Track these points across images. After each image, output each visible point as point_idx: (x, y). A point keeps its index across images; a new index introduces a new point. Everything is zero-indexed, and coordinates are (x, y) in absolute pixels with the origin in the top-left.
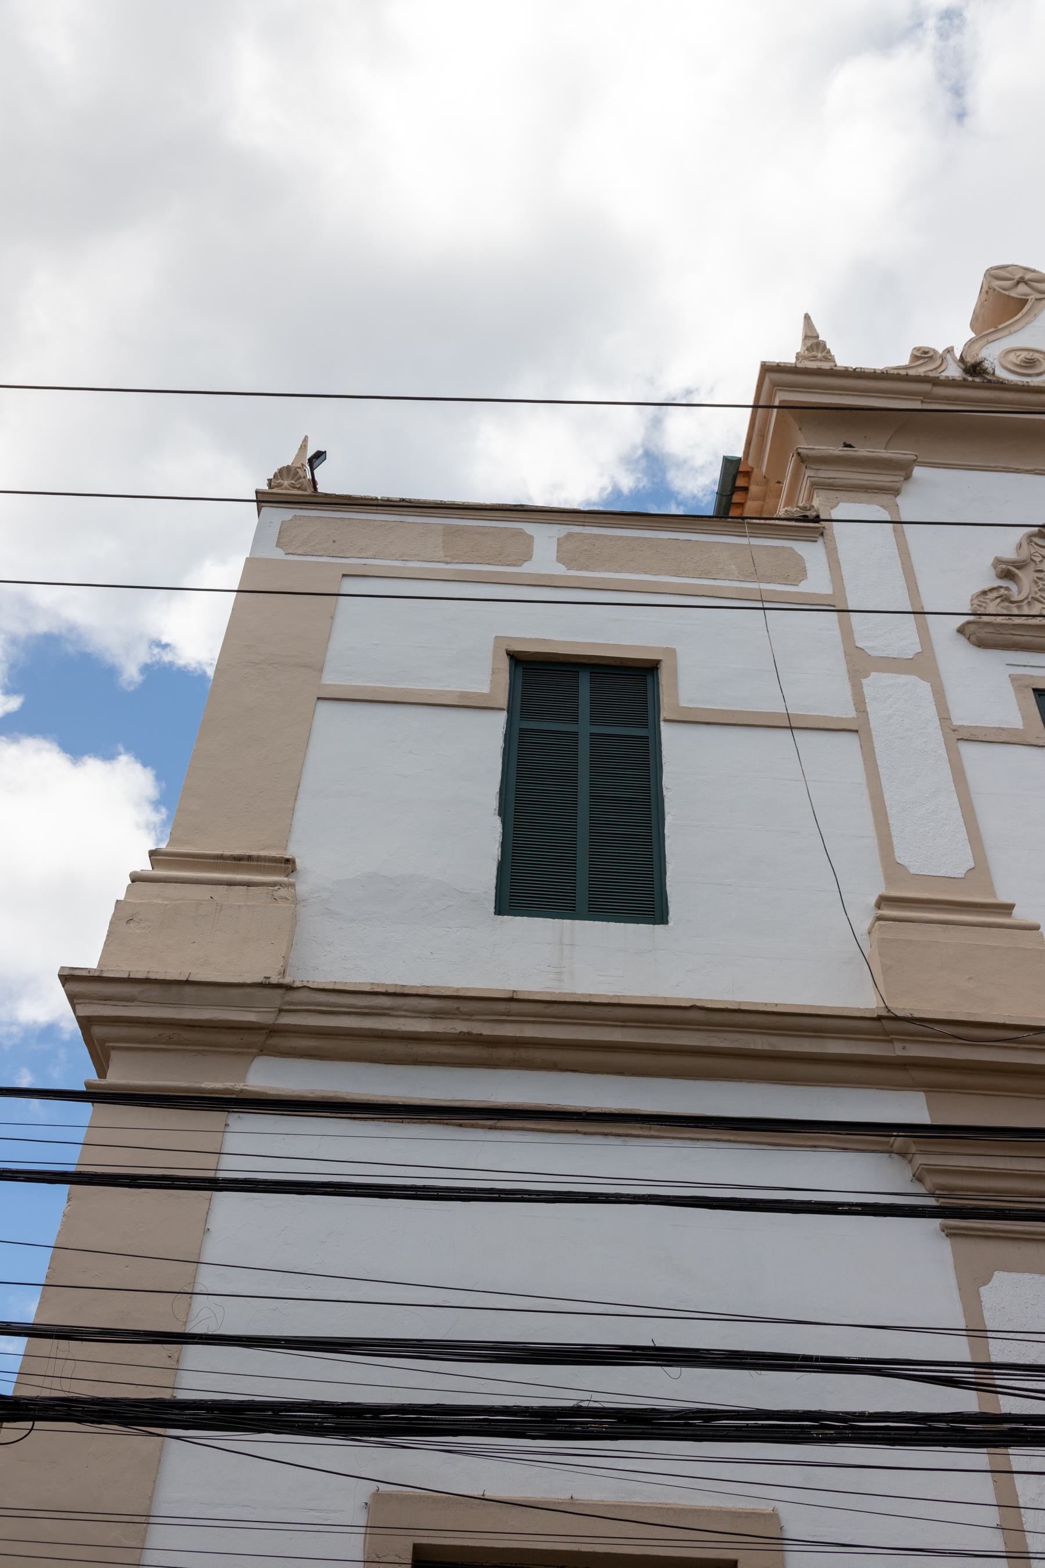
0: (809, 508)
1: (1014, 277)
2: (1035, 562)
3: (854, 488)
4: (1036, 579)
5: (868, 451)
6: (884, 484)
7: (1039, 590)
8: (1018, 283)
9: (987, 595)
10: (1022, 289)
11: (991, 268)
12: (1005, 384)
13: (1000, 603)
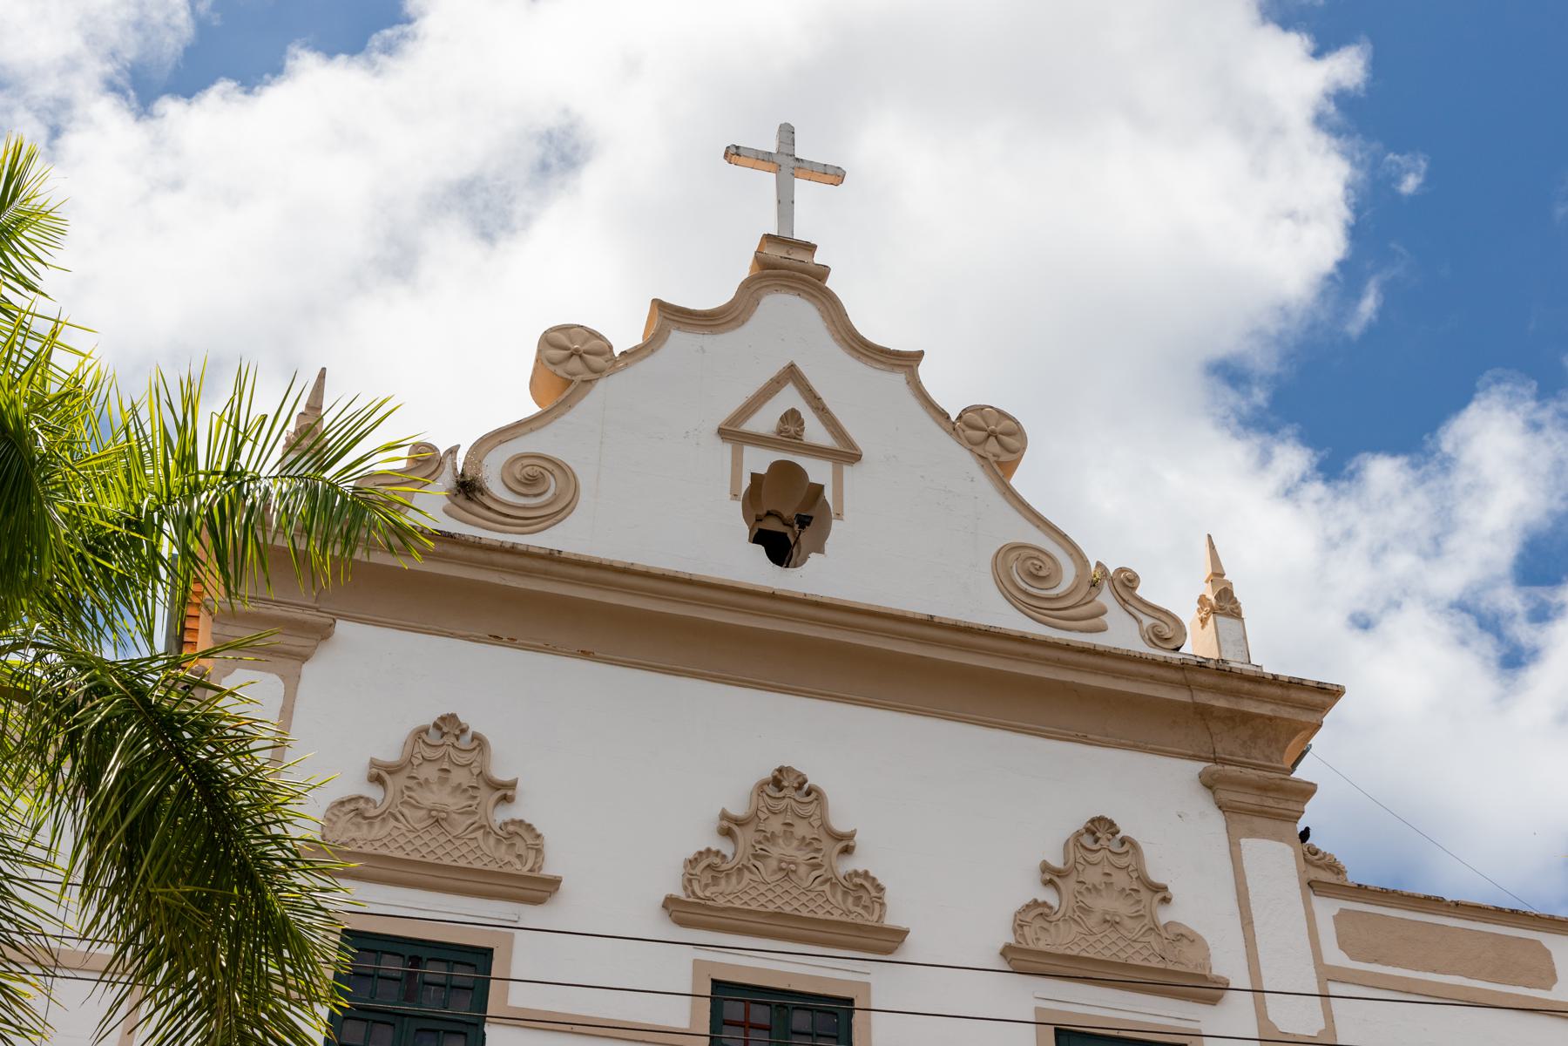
1: (570, 346)
2: (413, 765)
4: (404, 788)
5: (282, 610)
7: (401, 803)
8: (572, 355)
9: (344, 806)
10: (575, 364)
11: (551, 329)
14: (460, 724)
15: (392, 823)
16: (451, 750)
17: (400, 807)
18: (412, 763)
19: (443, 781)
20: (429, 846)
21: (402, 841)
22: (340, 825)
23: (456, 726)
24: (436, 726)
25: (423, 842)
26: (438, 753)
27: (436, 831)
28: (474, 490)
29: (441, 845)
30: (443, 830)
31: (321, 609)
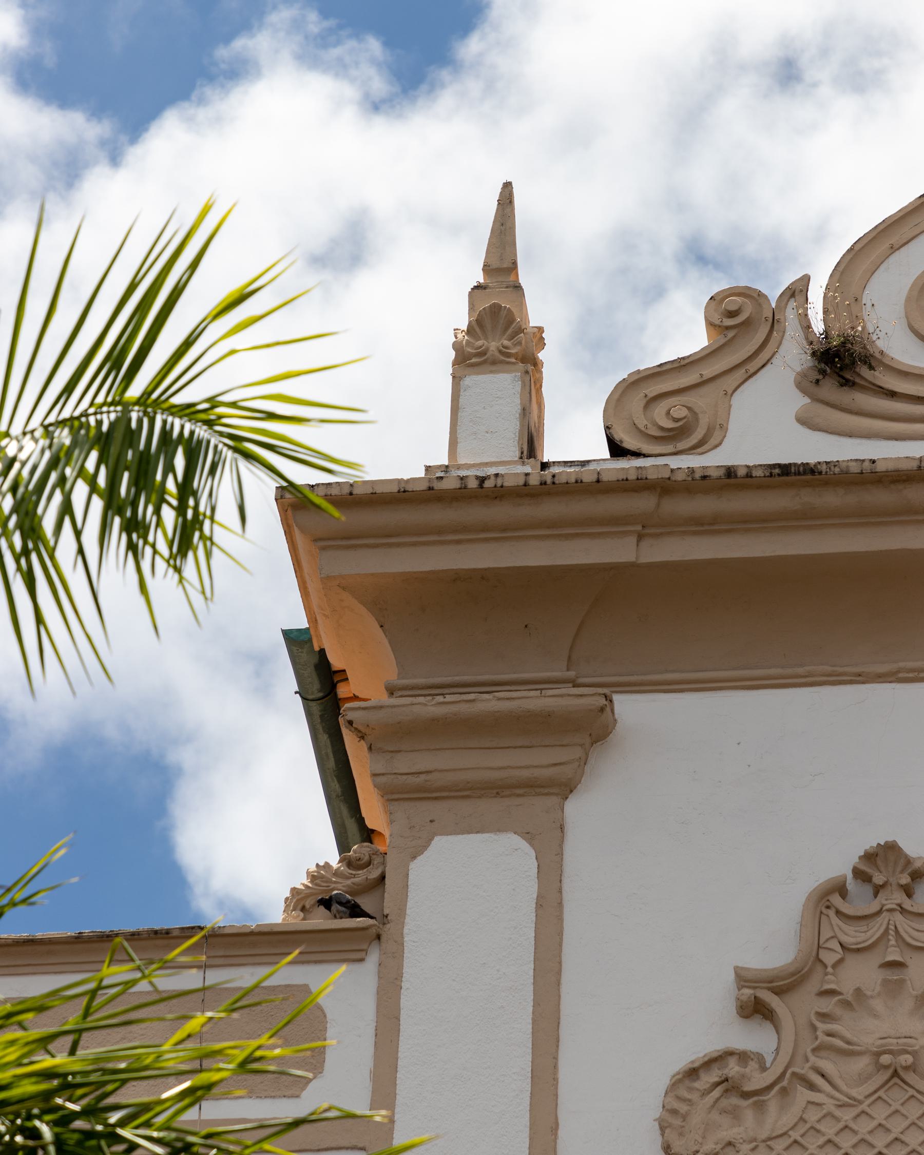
0: (366, 858)
2: (826, 966)
3: (470, 789)
4: (813, 1018)
5: (499, 699)
6: (537, 773)
7: (814, 1050)
12: (820, 473)
13: (718, 1099)
14: (908, 861)
15: (803, 1095)
16: (898, 918)
17: (812, 1059)
18: (821, 961)
19: (893, 989)
20: (888, 1130)
21: (829, 1129)
22: (696, 1119)
23: (899, 869)
24: (858, 874)
25: (875, 1123)
26: (875, 930)
27: (897, 1096)
28: (854, 363)
29: (914, 1124)
30: (911, 1092)
31: (581, 680)
